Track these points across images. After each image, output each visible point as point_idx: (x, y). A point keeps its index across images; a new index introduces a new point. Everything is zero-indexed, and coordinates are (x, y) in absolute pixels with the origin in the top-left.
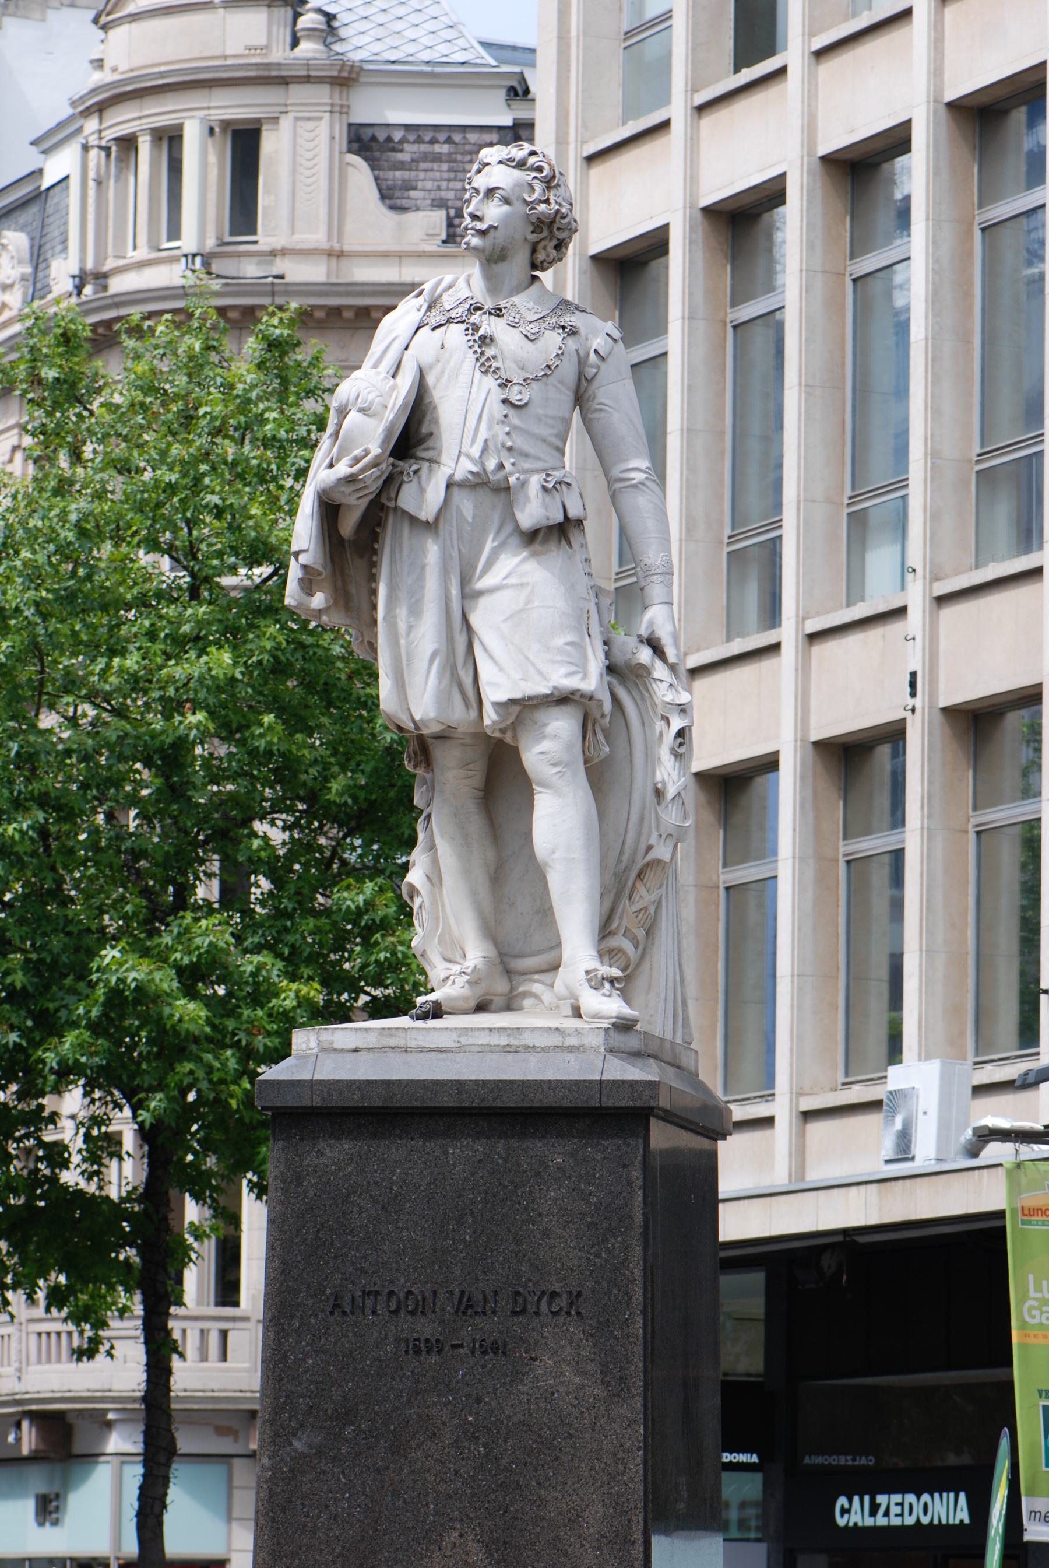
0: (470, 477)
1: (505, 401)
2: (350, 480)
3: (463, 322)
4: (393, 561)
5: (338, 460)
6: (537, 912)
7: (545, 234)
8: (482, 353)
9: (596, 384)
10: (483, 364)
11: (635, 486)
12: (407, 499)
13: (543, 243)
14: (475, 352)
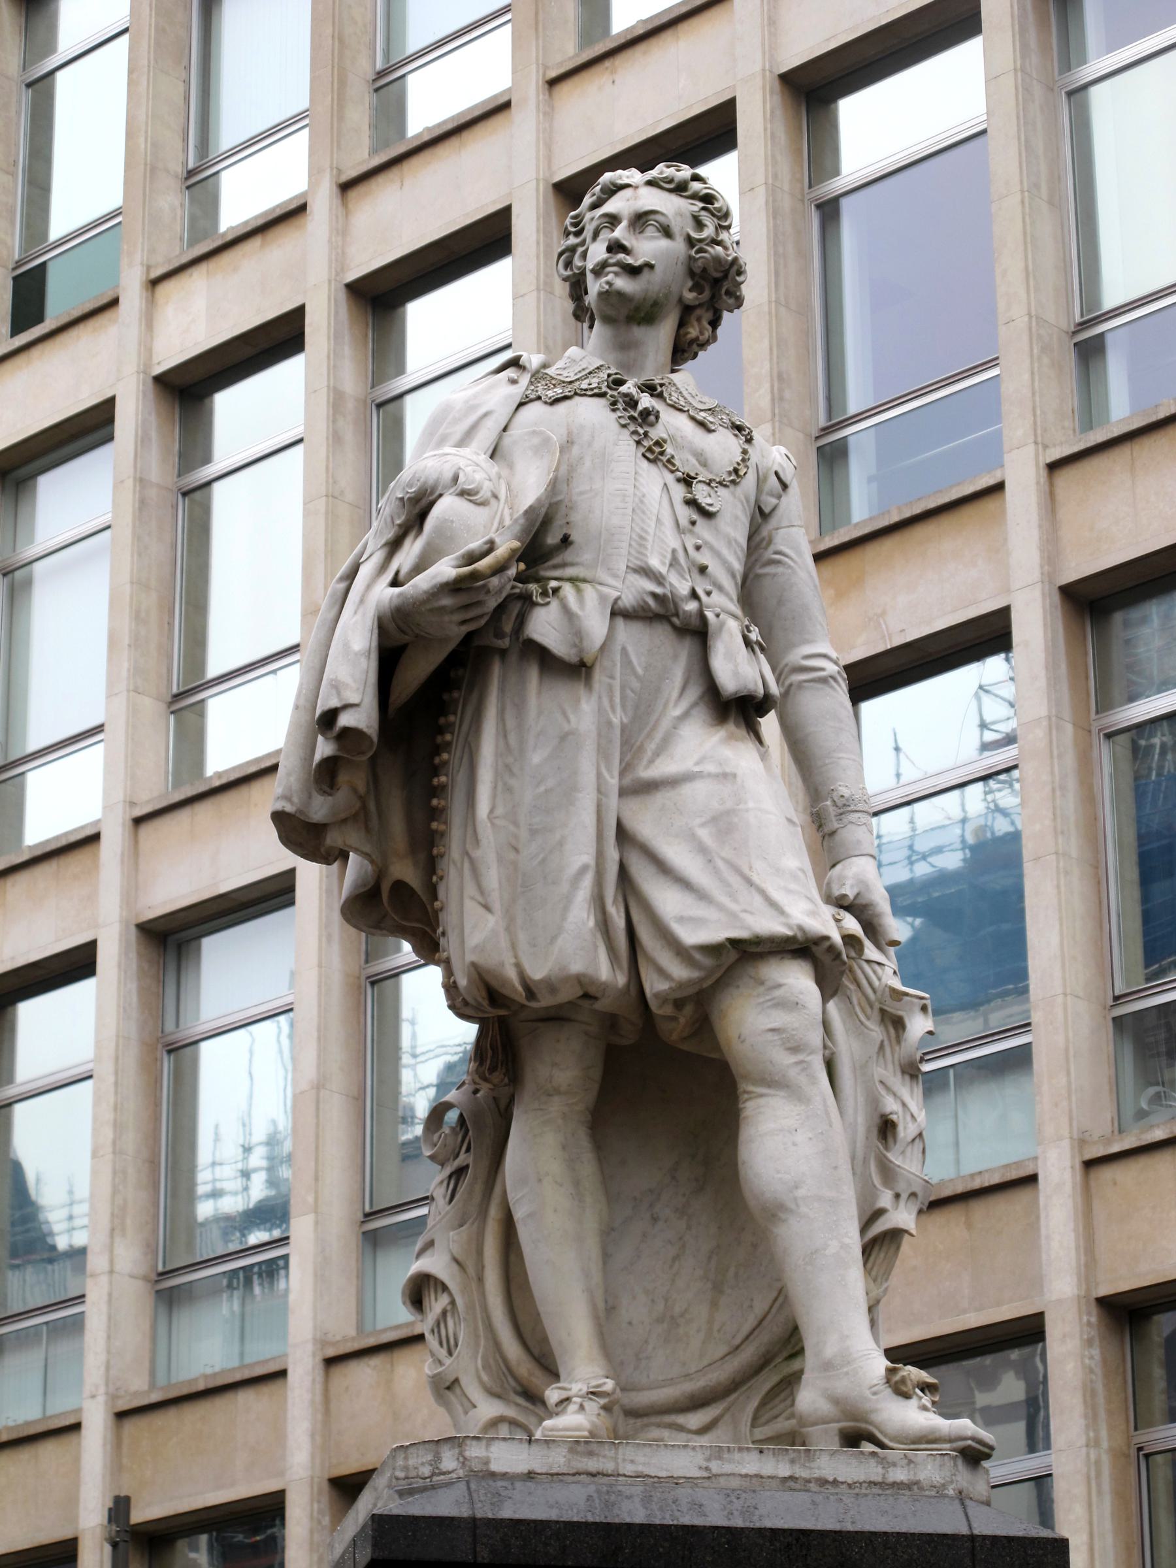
0: (651, 602)
1: (692, 503)
3: (602, 395)
4: (503, 733)
6: (660, 1320)
7: (706, 295)
9: (773, 522)
10: (650, 450)
12: (545, 626)
13: (698, 312)
14: (635, 432)
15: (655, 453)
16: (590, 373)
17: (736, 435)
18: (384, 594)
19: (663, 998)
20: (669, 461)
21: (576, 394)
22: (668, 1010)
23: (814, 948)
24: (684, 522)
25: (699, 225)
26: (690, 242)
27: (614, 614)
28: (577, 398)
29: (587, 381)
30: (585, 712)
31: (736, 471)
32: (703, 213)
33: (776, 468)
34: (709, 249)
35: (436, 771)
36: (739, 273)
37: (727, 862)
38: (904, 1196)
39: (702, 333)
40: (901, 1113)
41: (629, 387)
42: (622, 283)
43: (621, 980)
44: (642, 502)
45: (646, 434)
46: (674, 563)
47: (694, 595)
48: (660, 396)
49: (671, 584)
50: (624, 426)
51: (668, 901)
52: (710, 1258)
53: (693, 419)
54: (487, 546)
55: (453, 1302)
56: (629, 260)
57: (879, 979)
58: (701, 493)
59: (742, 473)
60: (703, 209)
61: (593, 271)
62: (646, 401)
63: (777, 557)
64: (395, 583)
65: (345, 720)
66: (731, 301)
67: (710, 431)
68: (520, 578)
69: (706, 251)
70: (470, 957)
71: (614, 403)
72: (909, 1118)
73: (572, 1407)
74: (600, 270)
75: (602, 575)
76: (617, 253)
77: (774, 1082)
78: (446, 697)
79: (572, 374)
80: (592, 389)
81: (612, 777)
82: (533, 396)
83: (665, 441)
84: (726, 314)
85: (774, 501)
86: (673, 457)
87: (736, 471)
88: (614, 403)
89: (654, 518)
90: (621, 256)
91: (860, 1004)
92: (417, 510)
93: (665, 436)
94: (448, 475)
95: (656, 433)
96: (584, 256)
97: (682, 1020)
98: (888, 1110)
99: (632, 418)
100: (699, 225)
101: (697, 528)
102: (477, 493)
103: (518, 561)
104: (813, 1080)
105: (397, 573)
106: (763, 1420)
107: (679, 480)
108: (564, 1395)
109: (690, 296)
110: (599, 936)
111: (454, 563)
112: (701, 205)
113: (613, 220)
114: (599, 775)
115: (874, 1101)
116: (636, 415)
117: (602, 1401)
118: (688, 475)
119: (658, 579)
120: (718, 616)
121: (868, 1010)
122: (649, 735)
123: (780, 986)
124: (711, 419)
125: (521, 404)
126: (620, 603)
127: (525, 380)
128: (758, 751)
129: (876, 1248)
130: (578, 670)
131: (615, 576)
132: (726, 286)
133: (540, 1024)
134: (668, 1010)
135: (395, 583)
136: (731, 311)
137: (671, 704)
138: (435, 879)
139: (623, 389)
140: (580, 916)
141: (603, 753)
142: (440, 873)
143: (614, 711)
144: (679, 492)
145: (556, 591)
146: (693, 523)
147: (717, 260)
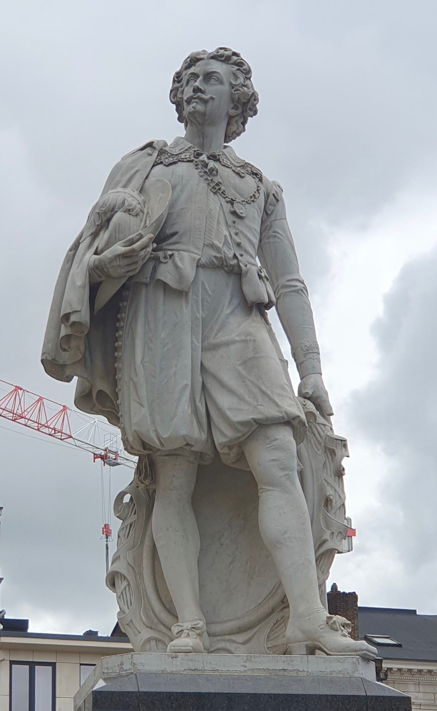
1: (234, 213)
2: (124, 256)
3: (191, 161)
5: (108, 245)
7: (240, 111)
8: (212, 180)
9: (272, 218)
10: (214, 188)
11: (297, 291)
12: (166, 273)
13: (236, 118)
14: (207, 179)
15: (217, 189)
16: (186, 150)
17: (254, 178)
18: (90, 258)
19: (224, 445)
20: (222, 193)
21: (179, 161)
22: (226, 451)
23: (292, 421)
24: (230, 222)
25: (236, 78)
26: (232, 86)
27: (197, 266)
28: (179, 163)
29: (184, 154)
30: (186, 312)
31: (254, 195)
32: (238, 71)
33: (273, 192)
34: (241, 89)
35: (116, 340)
36: (255, 100)
37: (252, 382)
38: (336, 533)
39: (238, 128)
40: (334, 495)
41: (204, 157)
42: (200, 107)
43: (204, 436)
44: (210, 213)
45: (212, 180)
46: (226, 243)
47: (235, 256)
48: (218, 160)
49: (224, 252)
50: (202, 176)
51: (224, 401)
52: (247, 563)
53: (234, 171)
54: (138, 237)
55: (129, 585)
56: (203, 96)
57: (323, 432)
58: (238, 208)
59: (257, 197)
60: (238, 69)
61: (186, 101)
62: (212, 164)
63: (274, 234)
64: (96, 253)
65: (73, 318)
66: (251, 113)
67: (242, 177)
68: (154, 250)
69: (239, 90)
70: (134, 428)
71: (197, 165)
72: (338, 496)
73: (183, 635)
74: (189, 102)
76: (197, 93)
77: (273, 484)
78: (121, 305)
79: (177, 151)
80: (186, 158)
81: (198, 343)
82: (159, 162)
83: (221, 183)
84: (249, 118)
85: (274, 208)
86: (224, 191)
87: (254, 195)
88: (197, 165)
89: (216, 221)
90: (199, 94)
91: (314, 443)
92: (104, 219)
93: (220, 181)
94: (120, 201)
95: (217, 179)
96: (182, 92)
97: (232, 455)
98: (328, 494)
99: (205, 172)
101: (236, 225)
102: (133, 210)
103: (153, 242)
104: (293, 484)
105: (97, 248)
106: (272, 638)
107: (227, 202)
108: (180, 629)
109: (232, 112)
110: (193, 416)
111: (123, 245)
112: (237, 68)
113: (195, 76)
114: (192, 342)
115: (322, 489)
116: (207, 170)
117: (198, 632)
118: (232, 199)
119: (218, 250)
120: (246, 266)
121: (319, 447)
123: (276, 439)
124: (242, 171)
125: (154, 166)
126: (201, 261)
127: (156, 154)
128: (266, 327)
129: (323, 557)
130: (181, 294)
131: (198, 248)
132: (249, 105)
133: (167, 457)
134: (226, 451)
135: (96, 253)
136: (252, 117)
137: (225, 308)
138: (117, 390)
139: (201, 158)
140: (184, 407)
141: (193, 332)
142: (119, 387)
143: (199, 312)
144: (228, 207)
145: (171, 256)
146: (234, 222)
147: (244, 93)
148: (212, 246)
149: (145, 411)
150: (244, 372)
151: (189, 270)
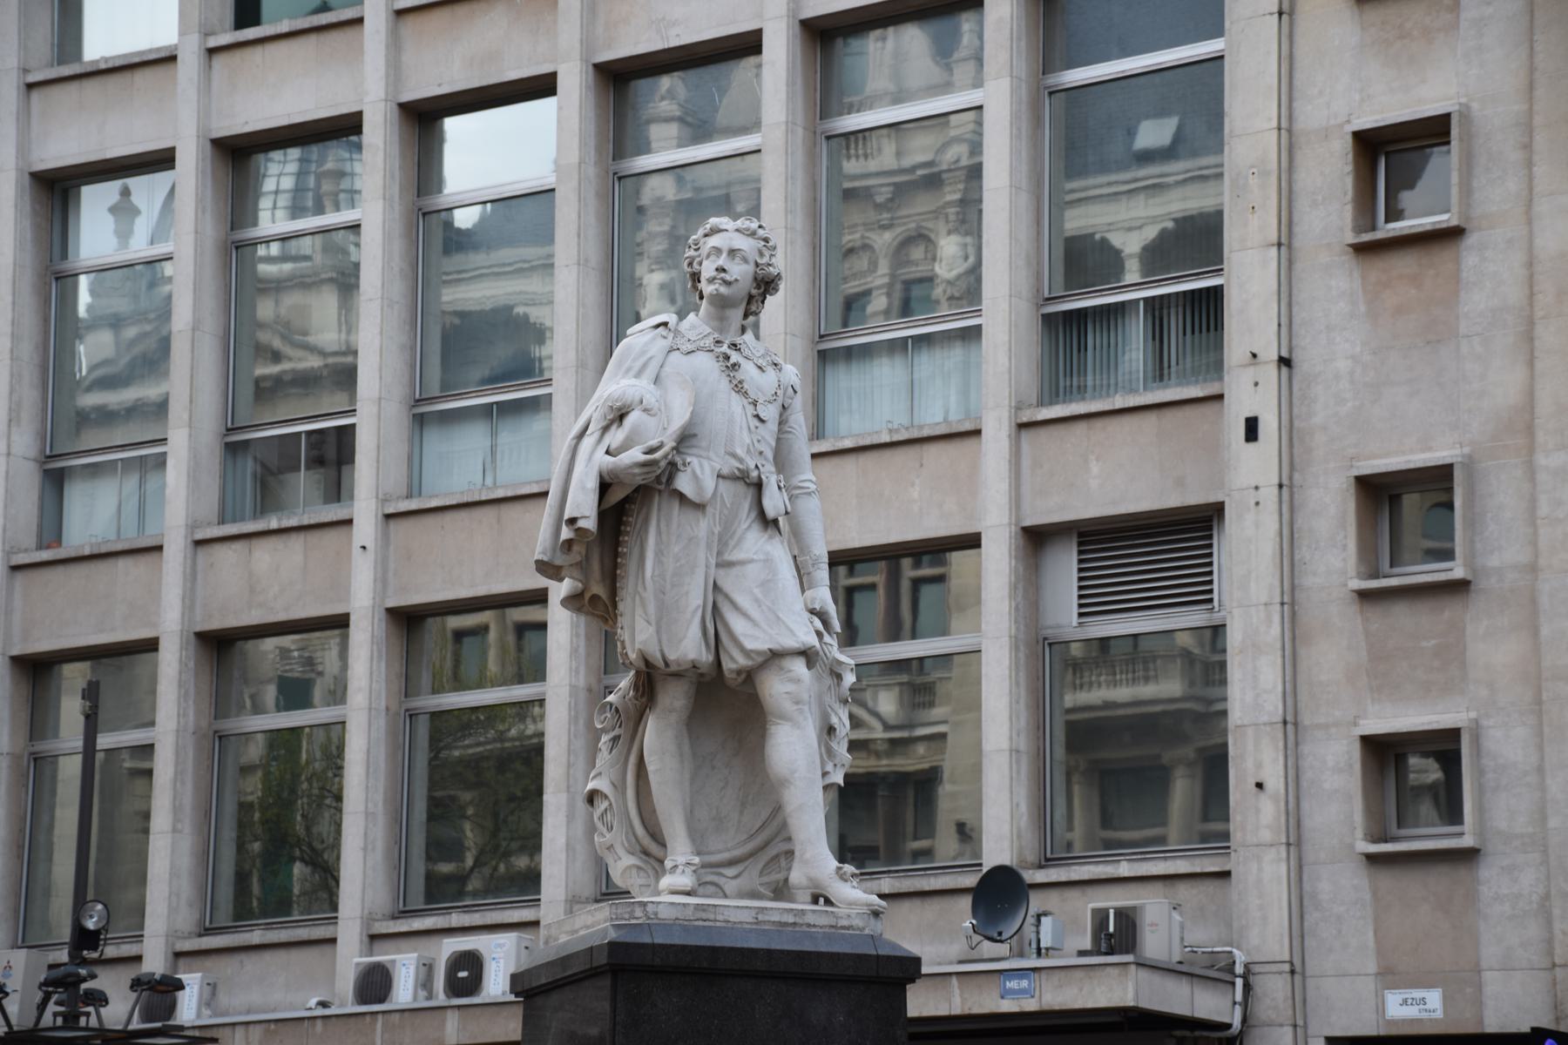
2: (644, 464)
4: (659, 532)
15: (739, 388)
18: (602, 460)
19: (732, 671)
25: (761, 254)
26: (757, 265)
41: (725, 348)
42: (723, 290)
43: (711, 658)
46: (748, 451)
51: (738, 625)
62: (735, 357)
64: (607, 452)
70: (637, 646)
74: (711, 281)
75: (711, 454)
77: (785, 717)
96: (700, 264)
100: (761, 254)
109: (754, 292)
113: (718, 251)
119: (741, 460)
122: (731, 537)
130: (700, 507)
141: (709, 547)
148: (734, 456)
149: (652, 630)
150: (760, 596)
151: (709, 483)
